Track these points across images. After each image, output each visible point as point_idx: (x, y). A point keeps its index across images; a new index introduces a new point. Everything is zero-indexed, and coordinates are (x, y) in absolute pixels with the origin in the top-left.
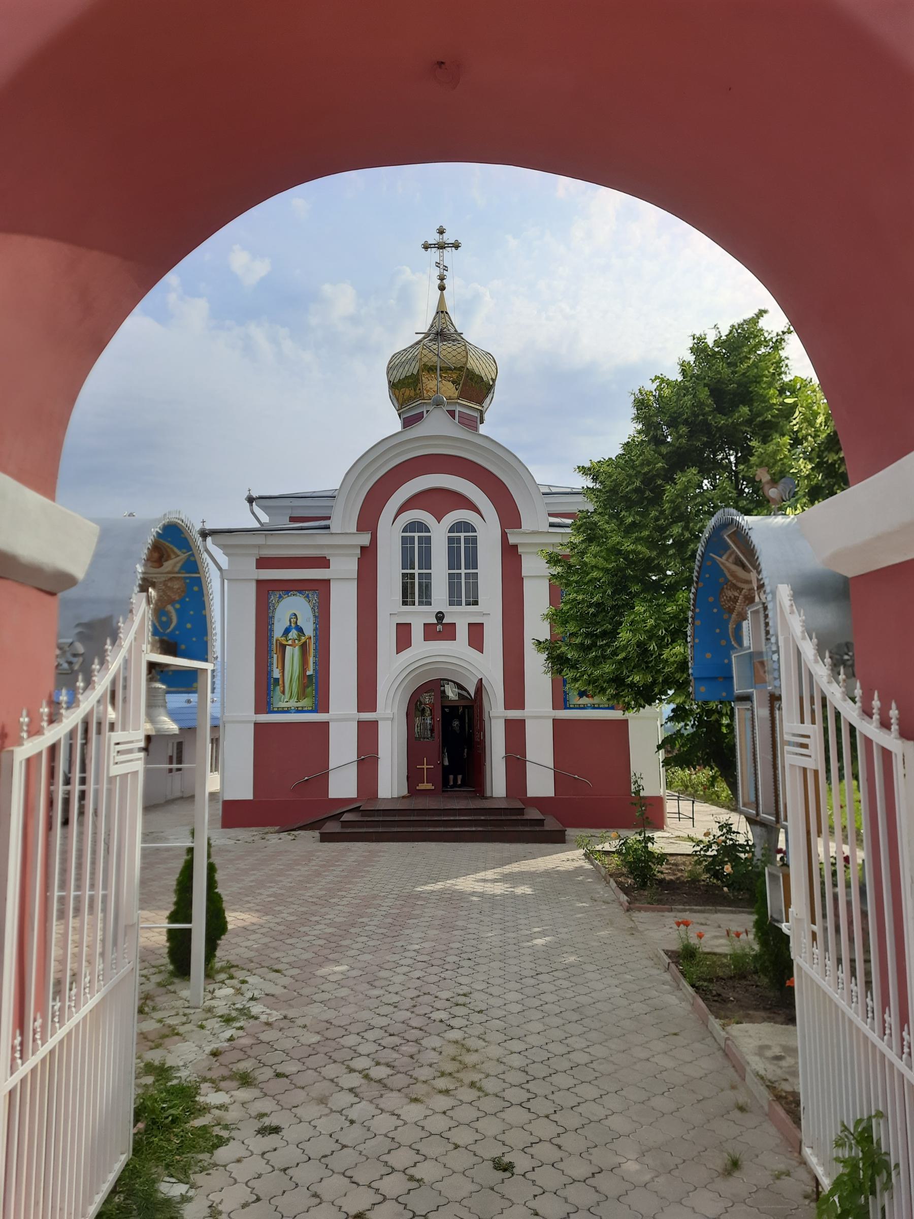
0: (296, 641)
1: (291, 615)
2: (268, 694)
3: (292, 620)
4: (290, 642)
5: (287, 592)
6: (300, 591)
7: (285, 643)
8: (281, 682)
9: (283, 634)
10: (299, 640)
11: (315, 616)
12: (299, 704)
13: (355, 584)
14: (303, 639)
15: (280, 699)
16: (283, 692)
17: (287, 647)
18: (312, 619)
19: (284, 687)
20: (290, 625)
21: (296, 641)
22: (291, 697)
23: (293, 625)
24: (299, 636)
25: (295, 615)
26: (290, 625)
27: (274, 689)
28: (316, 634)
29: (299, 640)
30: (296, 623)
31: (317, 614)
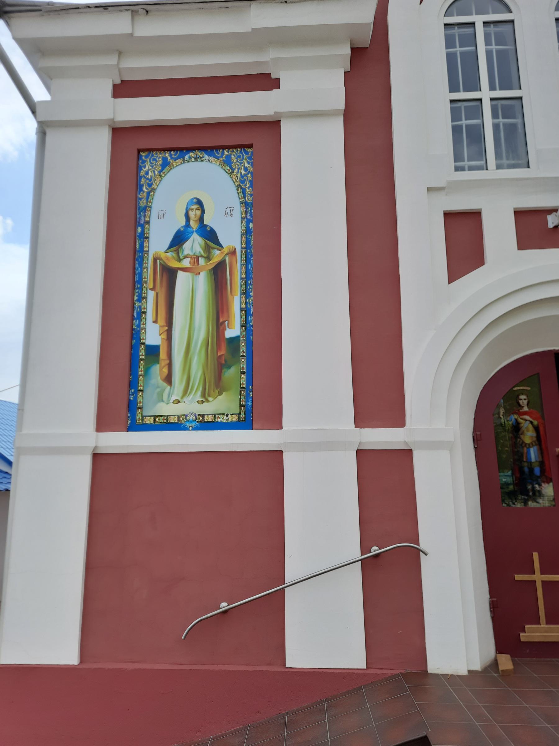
0: (202, 261)
1: (191, 202)
2: (132, 384)
3: (192, 214)
4: (186, 263)
5: (182, 151)
6: (210, 149)
7: (174, 264)
8: (163, 355)
9: (171, 246)
10: (208, 258)
11: (245, 204)
12: (209, 408)
13: (342, 118)
14: (217, 256)
15: (161, 394)
16: (169, 379)
17: (180, 274)
18: (238, 211)
19: (170, 365)
20: (188, 225)
21: (202, 261)
22: (186, 392)
23: (194, 225)
24: (208, 249)
25: (199, 203)
26: (188, 225)
27: (147, 370)
28: (248, 242)
29: (208, 258)
30: (201, 219)
31: (249, 199)
